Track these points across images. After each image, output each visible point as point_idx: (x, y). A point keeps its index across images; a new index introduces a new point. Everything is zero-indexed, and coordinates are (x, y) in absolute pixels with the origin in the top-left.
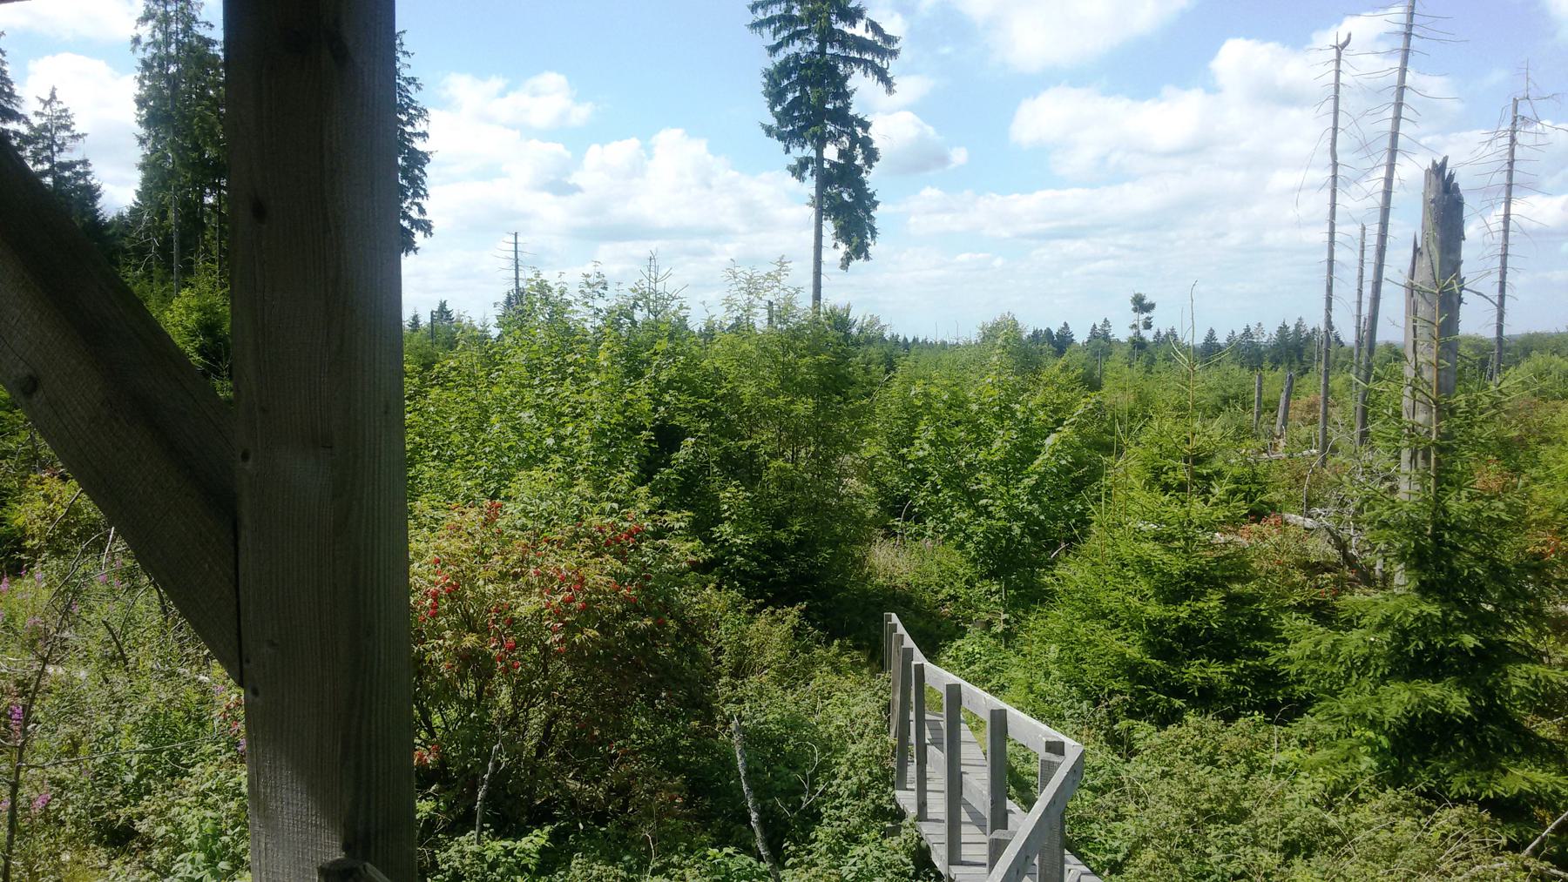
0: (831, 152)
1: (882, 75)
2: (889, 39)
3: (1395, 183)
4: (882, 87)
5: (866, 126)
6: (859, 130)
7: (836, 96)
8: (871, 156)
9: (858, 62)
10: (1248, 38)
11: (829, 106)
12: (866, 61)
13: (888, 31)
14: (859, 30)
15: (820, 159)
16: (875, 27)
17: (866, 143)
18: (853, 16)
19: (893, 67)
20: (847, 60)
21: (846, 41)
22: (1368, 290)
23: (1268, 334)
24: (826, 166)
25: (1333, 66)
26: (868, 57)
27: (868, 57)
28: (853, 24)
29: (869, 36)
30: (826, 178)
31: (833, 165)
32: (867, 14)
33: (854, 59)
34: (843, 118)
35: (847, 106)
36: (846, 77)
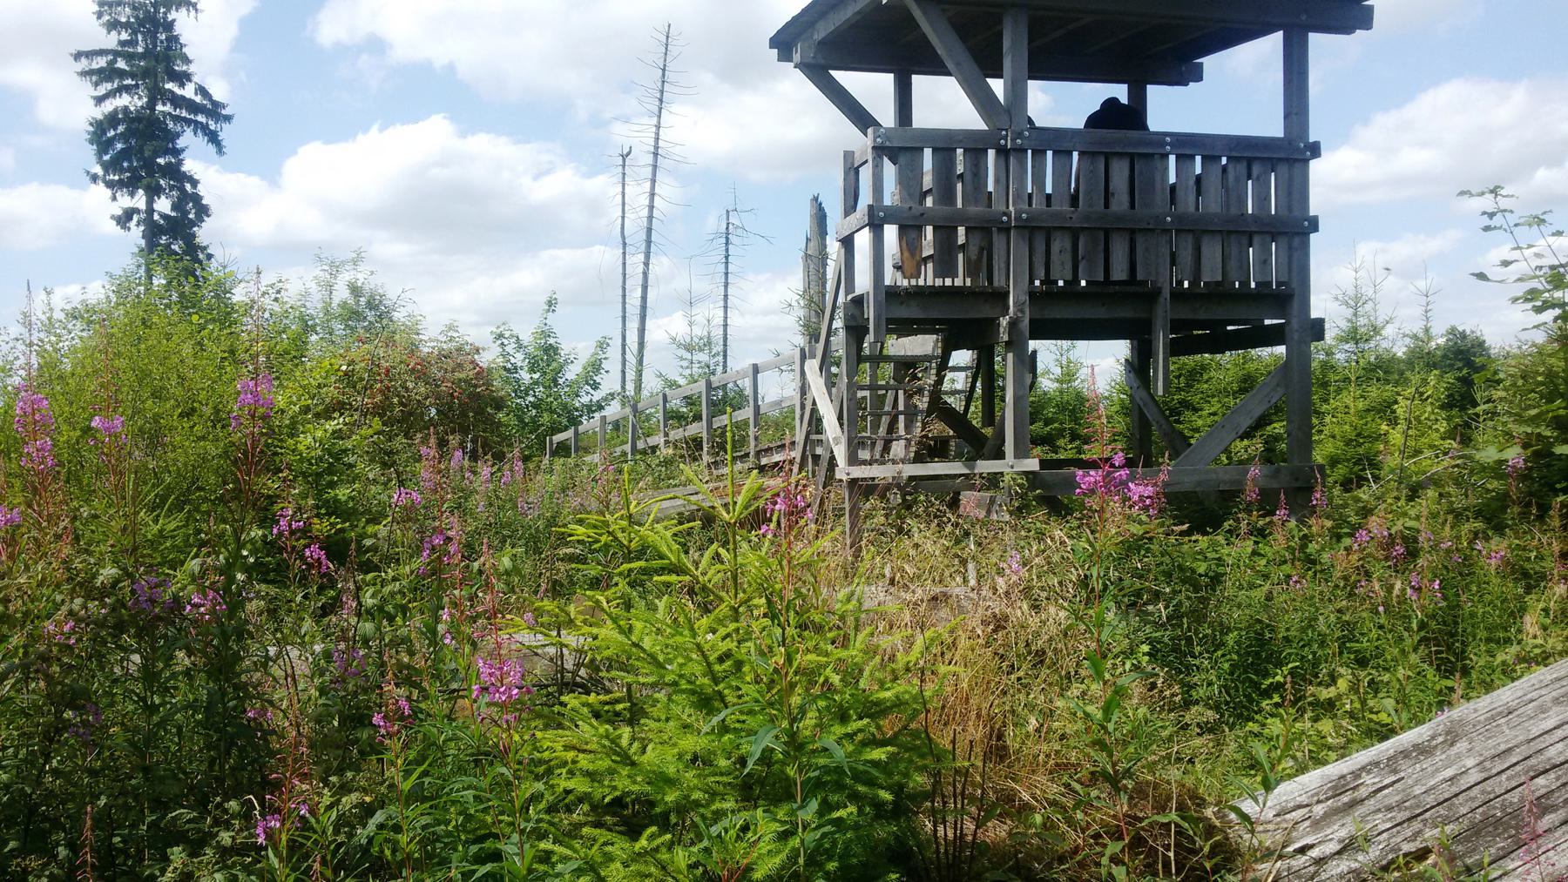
0: (163, 205)
1: (213, 138)
2: (216, 104)
3: (650, 277)
4: (212, 148)
5: (195, 183)
6: (188, 187)
7: (166, 152)
8: (203, 211)
9: (188, 122)
10: (488, 132)
11: (161, 161)
12: (196, 122)
13: (216, 97)
14: (188, 92)
15: (150, 210)
16: (201, 90)
17: (197, 199)
18: (183, 78)
19: (226, 132)
20: (177, 119)
21: (177, 101)
22: (631, 359)
23: (204, 202)
24: (156, 217)
25: (648, 185)
26: (201, 118)
27: (201, 118)
28: (182, 85)
29: (198, 99)
30: (153, 231)
31: (164, 216)
32: (195, 79)
33: (185, 120)
34: (176, 174)
35: (180, 162)
36: (178, 135)
